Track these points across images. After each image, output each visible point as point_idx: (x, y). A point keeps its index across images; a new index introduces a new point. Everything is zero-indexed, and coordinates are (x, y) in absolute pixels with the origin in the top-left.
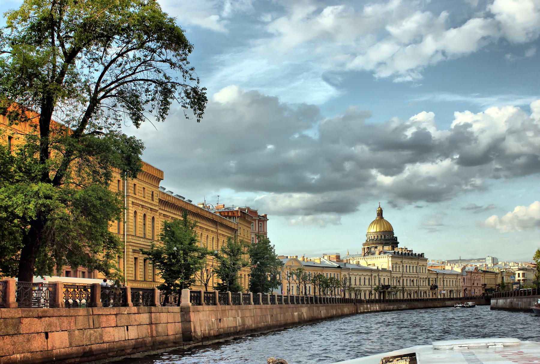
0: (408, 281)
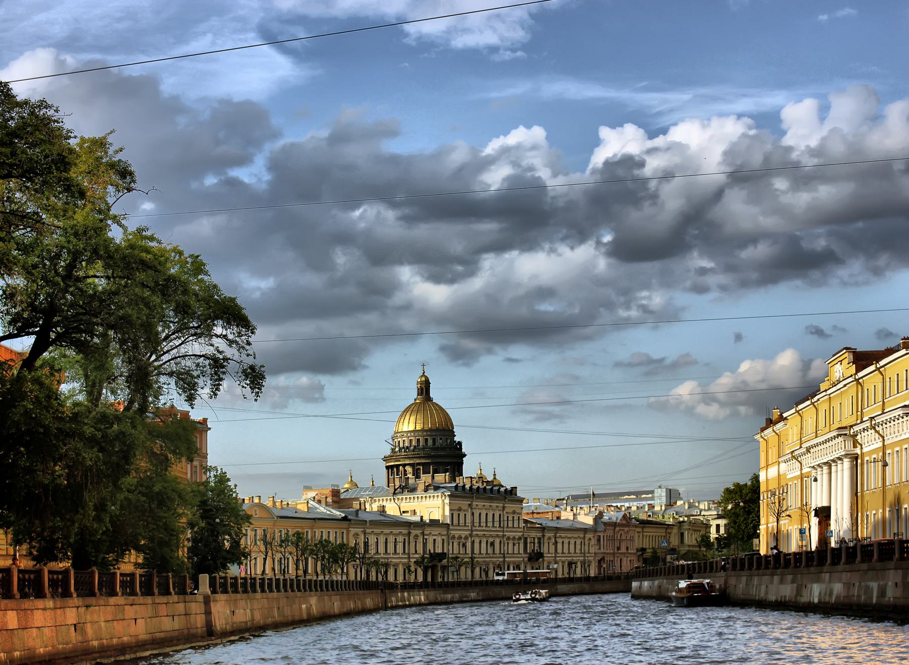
0: (484, 545)
